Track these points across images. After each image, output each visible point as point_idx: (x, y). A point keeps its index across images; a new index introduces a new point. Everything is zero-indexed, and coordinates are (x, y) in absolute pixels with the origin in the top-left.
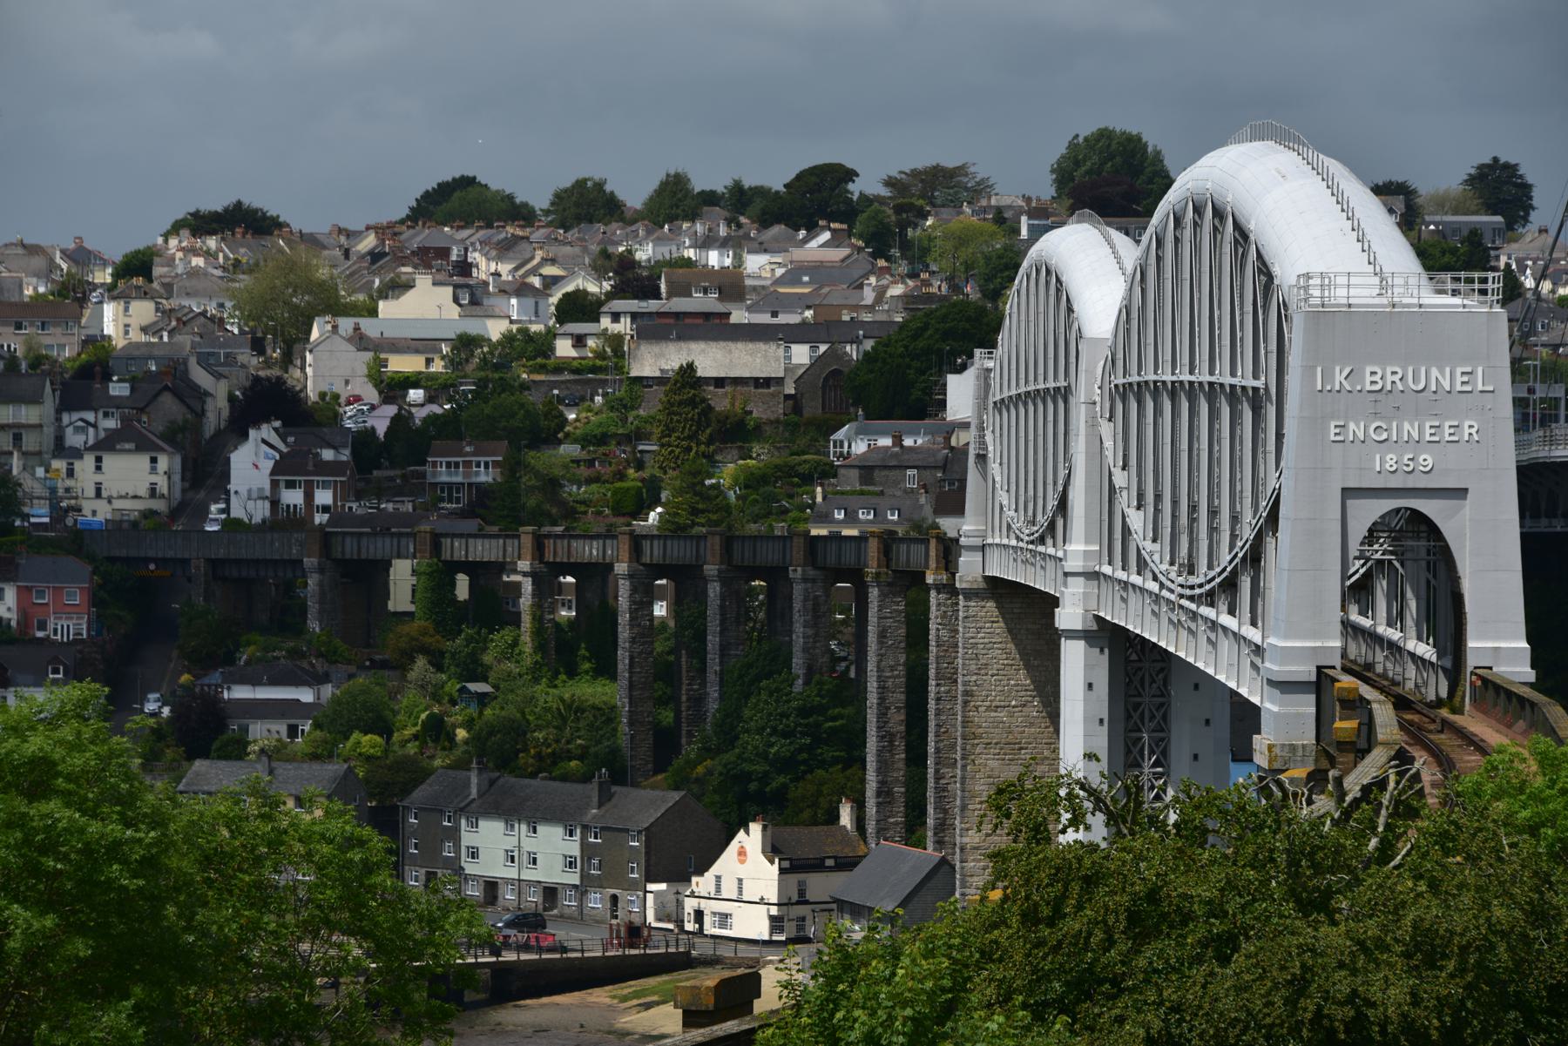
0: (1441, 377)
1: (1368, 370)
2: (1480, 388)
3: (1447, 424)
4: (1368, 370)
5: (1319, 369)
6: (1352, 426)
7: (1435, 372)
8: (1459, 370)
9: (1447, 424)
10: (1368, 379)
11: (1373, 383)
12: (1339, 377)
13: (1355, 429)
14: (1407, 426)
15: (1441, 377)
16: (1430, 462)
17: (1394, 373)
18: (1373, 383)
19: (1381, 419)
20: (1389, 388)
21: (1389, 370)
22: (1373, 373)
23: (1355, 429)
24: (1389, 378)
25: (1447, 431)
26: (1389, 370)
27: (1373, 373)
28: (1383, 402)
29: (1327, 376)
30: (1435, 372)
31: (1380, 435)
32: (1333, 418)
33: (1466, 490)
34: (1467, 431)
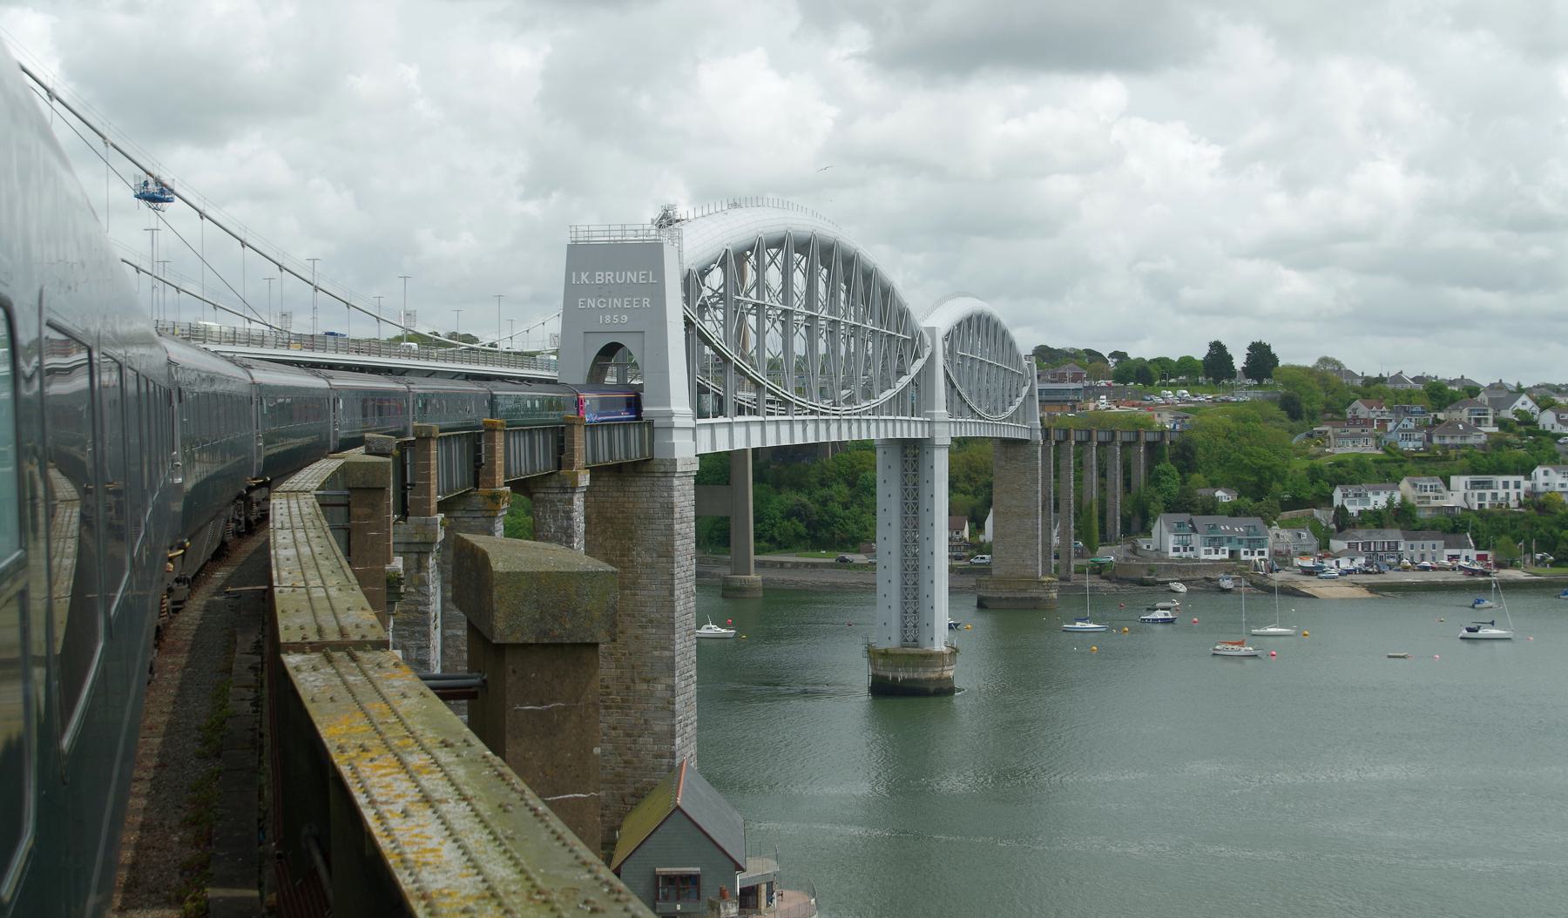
0: (632, 277)
1: (597, 273)
2: (651, 281)
3: (635, 299)
4: (597, 273)
5: (574, 274)
6: (589, 301)
7: (629, 274)
8: (641, 273)
9: (635, 299)
10: (597, 278)
11: (599, 280)
12: (584, 277)
13: (591, 303)
14: (615, 300)
15: (632, 277)
16: (626, 318)
17: (609, 275)
18: (599, 280)
19: (604, 297)
20: (607, 282)
21: (607, 273)
22: (599, 275)
23: (591, 303)
24: (607, 277)
25: (635, 303)
26: (607, 273)
27: (599, 275)
28: (603, 291)
29: (578, 278)
30: (629, 274)
31: (602, 305)
32: (580, 298)
33: (643, 332)
34: (644, 303)
